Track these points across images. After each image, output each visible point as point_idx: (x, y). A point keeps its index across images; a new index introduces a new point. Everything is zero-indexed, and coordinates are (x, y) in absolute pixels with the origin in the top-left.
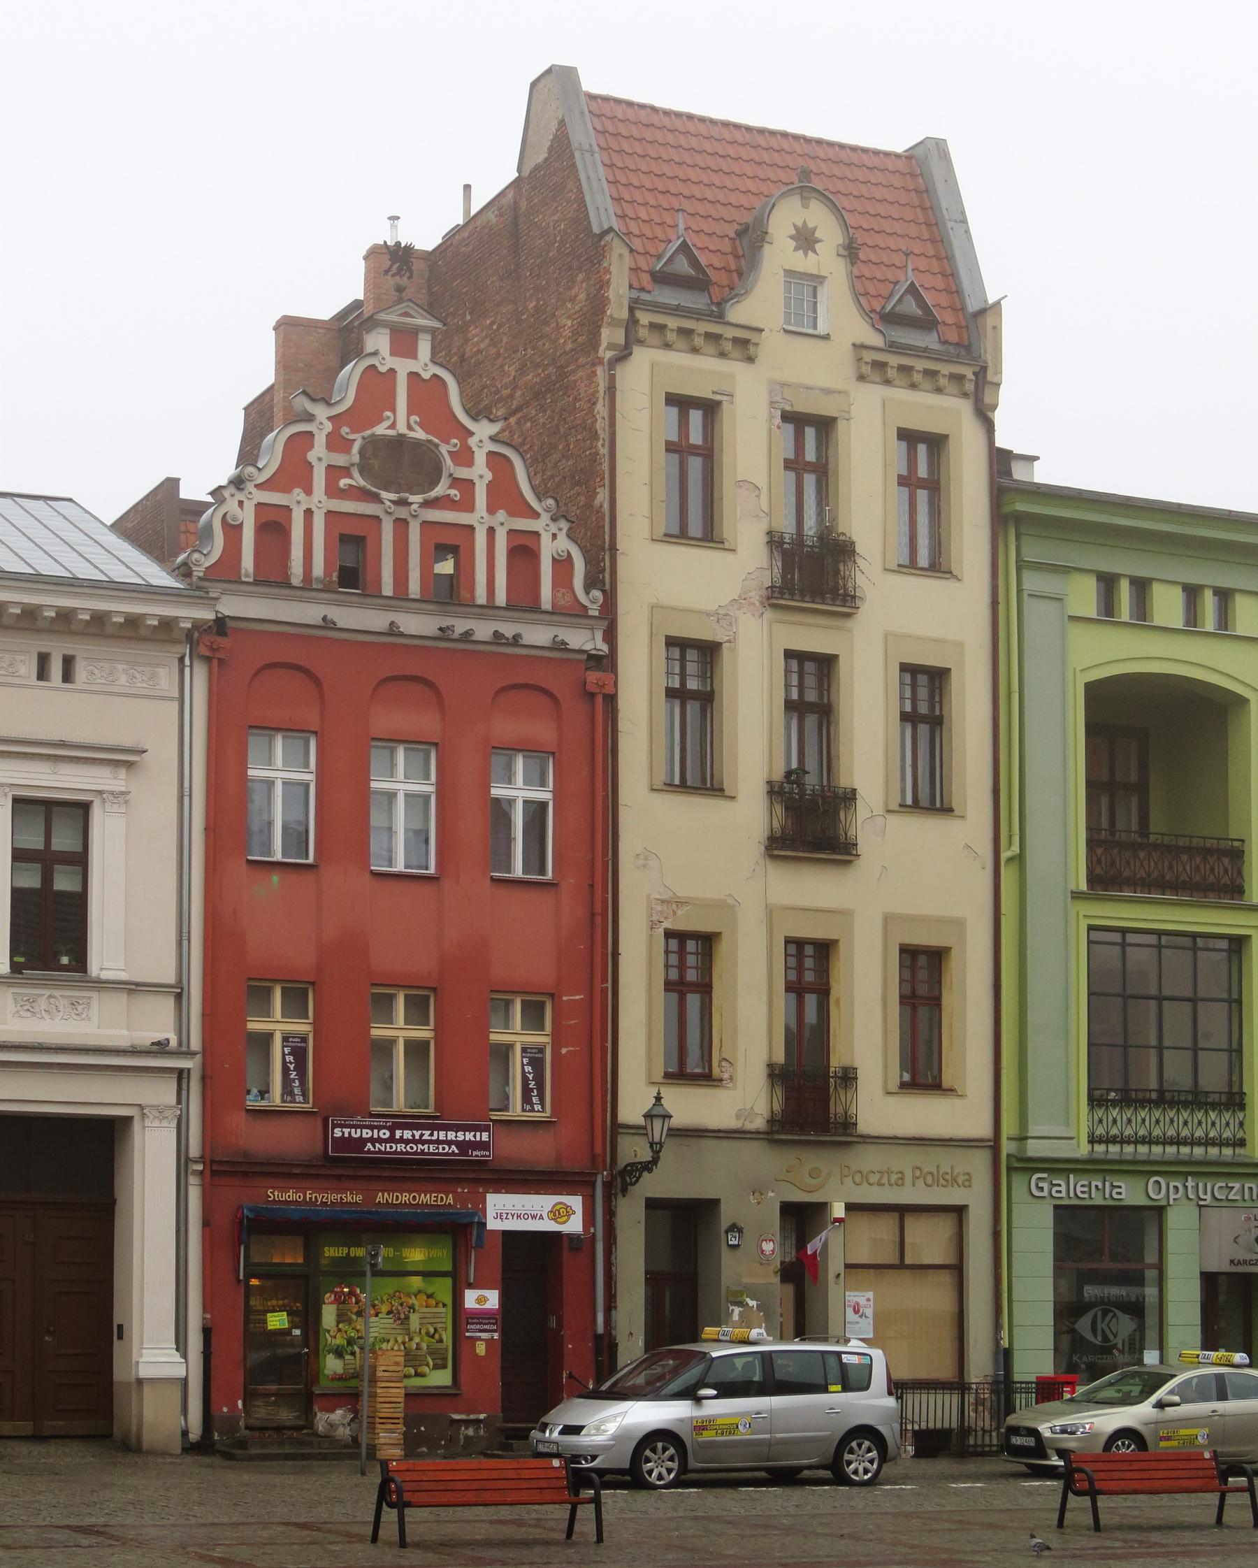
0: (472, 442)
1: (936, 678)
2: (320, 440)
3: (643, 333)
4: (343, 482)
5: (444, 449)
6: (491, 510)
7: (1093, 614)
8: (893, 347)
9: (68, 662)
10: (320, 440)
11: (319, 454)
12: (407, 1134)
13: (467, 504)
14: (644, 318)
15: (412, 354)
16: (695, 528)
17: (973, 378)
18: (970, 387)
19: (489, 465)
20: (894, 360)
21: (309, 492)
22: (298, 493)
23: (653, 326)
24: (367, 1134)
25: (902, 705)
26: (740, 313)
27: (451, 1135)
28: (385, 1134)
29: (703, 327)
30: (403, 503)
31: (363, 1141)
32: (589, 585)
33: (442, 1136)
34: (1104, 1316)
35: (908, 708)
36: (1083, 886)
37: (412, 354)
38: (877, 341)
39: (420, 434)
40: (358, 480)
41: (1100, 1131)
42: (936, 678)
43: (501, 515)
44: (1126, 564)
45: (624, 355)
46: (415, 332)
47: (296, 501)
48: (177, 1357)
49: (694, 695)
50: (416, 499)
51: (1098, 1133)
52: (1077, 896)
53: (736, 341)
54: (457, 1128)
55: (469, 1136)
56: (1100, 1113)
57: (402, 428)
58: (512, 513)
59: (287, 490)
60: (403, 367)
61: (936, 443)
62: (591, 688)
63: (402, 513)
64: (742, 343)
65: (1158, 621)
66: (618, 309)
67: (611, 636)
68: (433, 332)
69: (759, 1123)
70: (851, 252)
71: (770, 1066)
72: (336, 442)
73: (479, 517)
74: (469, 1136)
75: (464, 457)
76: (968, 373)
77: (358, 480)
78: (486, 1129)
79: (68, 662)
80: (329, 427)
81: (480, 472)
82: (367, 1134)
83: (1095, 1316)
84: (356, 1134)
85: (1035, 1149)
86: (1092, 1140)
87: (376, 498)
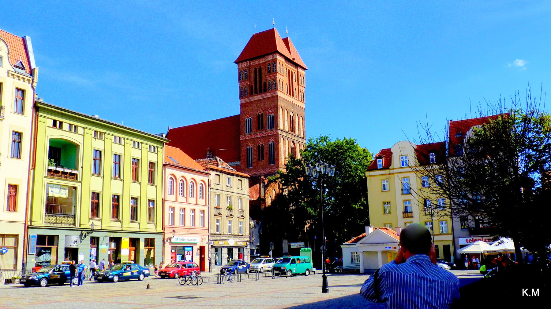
1: (20, 134)
7: (52, 126)
8: (16, 72)
17: (32, 80)
18: (31, 82)
20: (16, 74)
25: (13, 138)
34: (45, 256)
35: (14, 139)
36: (46, 175)
38: (13, 70)
41: (46, 221)
42: (20, 134)
44: (59, 119)
51: (46, 221)
52: (45, 177)
56: (47, 217)
61: (23, 91)
65: (64, 129)
70: (8, 53)
76: (31, 79)
83: (44, 256)
85: (33, 224)
86: (45, 223)
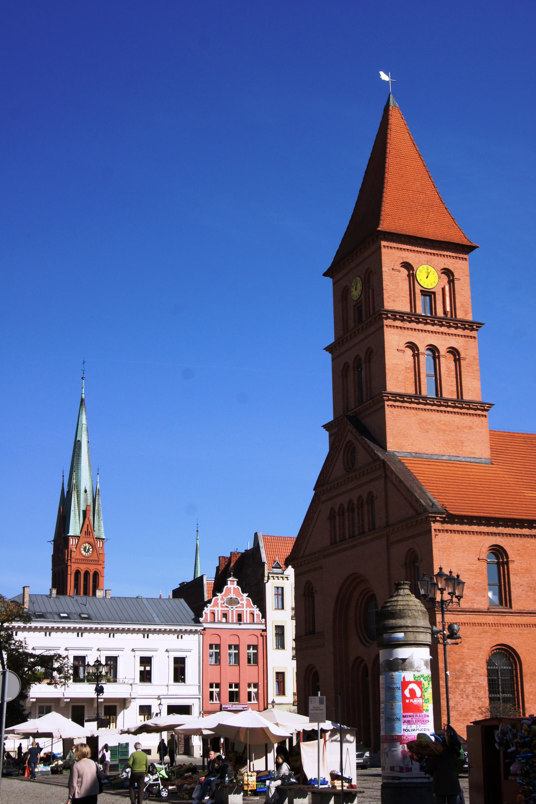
0: (243, 597)
2: (219, 599)
3: (270, 578)
4: (223, 605)
5: (239, 599)
6: (246, 608)
9: (182, 636)
10: (219, 599)
11: (220, 602)
12: (234, 706)
13: (243, 607)
14: (270, 575)
15: (234, 584)
16: (280, 607)
19: (246, 601)
21: (218, 607)
22: (216, 607)
23: (272, 577)
24: (228, 706)
26: (285, 573)
27: (241, 706)
28: (231, 706)
29: (280, 576)
30: (232, 608)
31: (227, 708)
32: (262, 618)
33: (240, 706)
37: (234, 584)
39: (235, 597)
40: (225, 605)
43: (248, 608)
45: (268, 581)
46: (234, 581)
47: (216, 609)
48: (199, 742)
49: (280, 634)
50: (234, 607)
53: (286, 577)
54: (242, 705)
55: (244, 706)
57: (232, 597)
58: (250, 608)
59: (215, 607)
60: (232, 587)
62: (262, 635)
63: (232, 609)
64: (287, 578)
66: (266, 575)
67: (266, 626)
68: (237, 581)
69: (292, 702)
71: (294, 693)
72: (222, 599)
73: (245, 609)
74: (244, 706)
75: (242, 600)
77: (225, 605)
78: (247, 705)
79: (182, 636)
80: (221, 597)
81: (245, 602)
82: (228, 706)
84: (226, 706)
87: (228, 607)
